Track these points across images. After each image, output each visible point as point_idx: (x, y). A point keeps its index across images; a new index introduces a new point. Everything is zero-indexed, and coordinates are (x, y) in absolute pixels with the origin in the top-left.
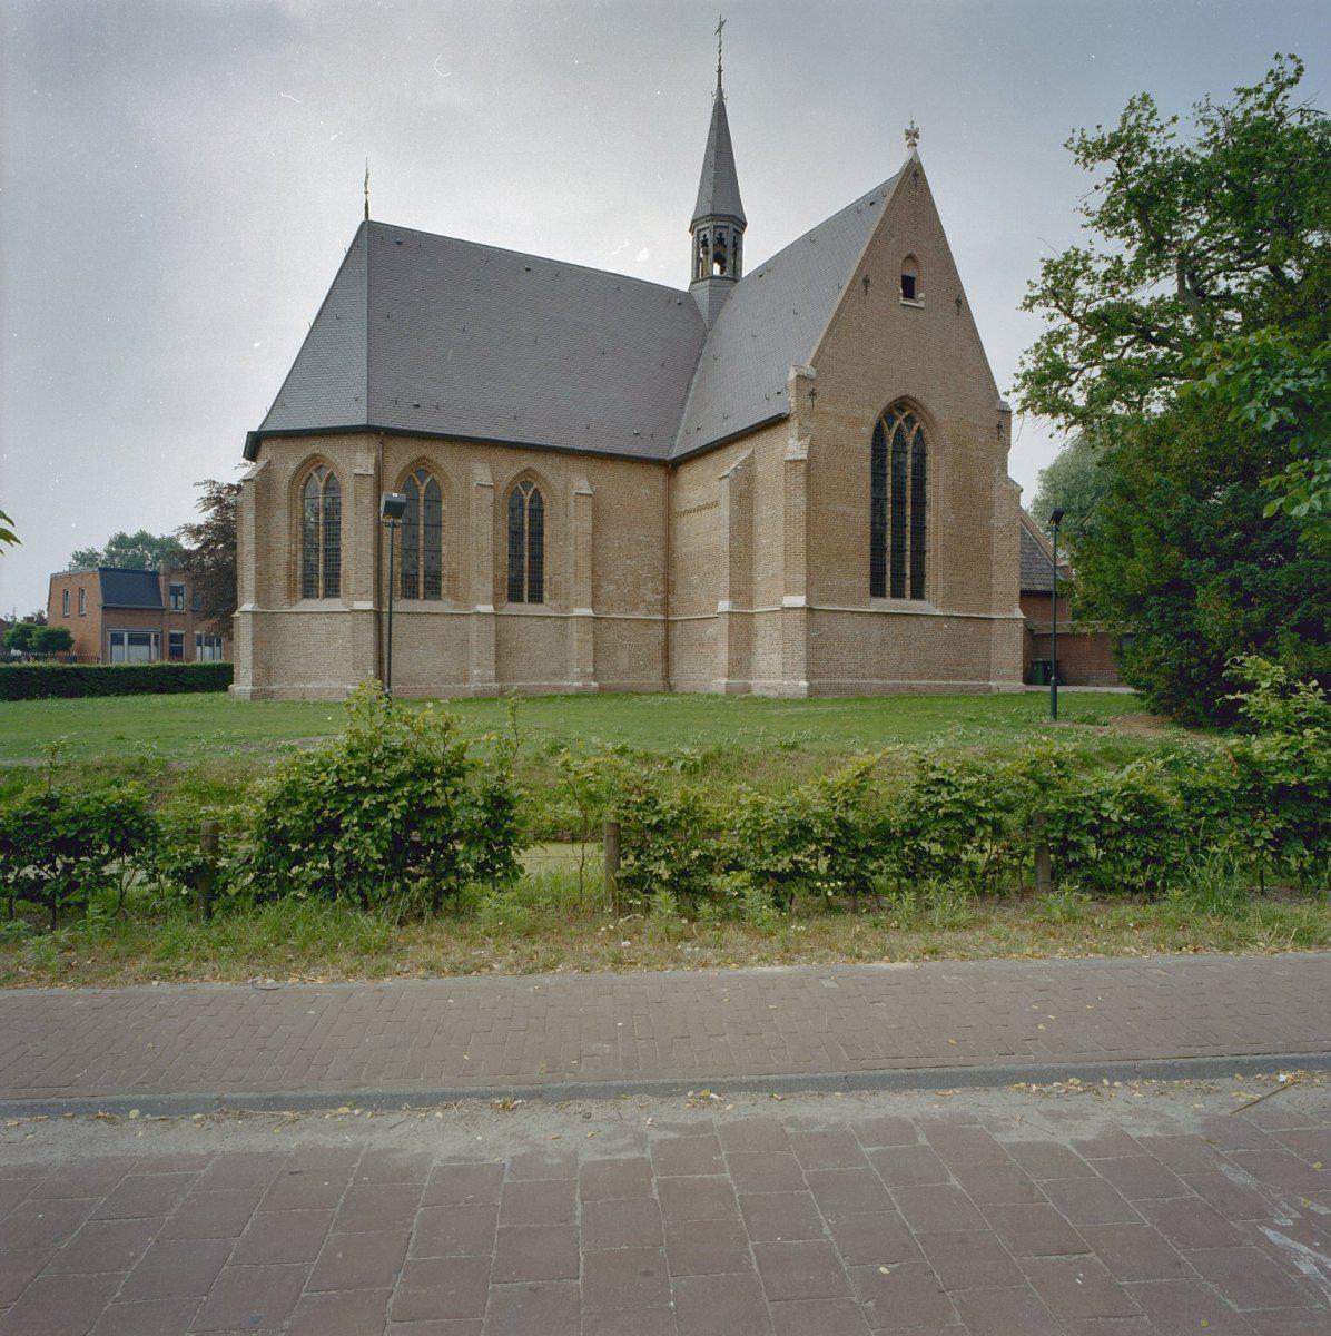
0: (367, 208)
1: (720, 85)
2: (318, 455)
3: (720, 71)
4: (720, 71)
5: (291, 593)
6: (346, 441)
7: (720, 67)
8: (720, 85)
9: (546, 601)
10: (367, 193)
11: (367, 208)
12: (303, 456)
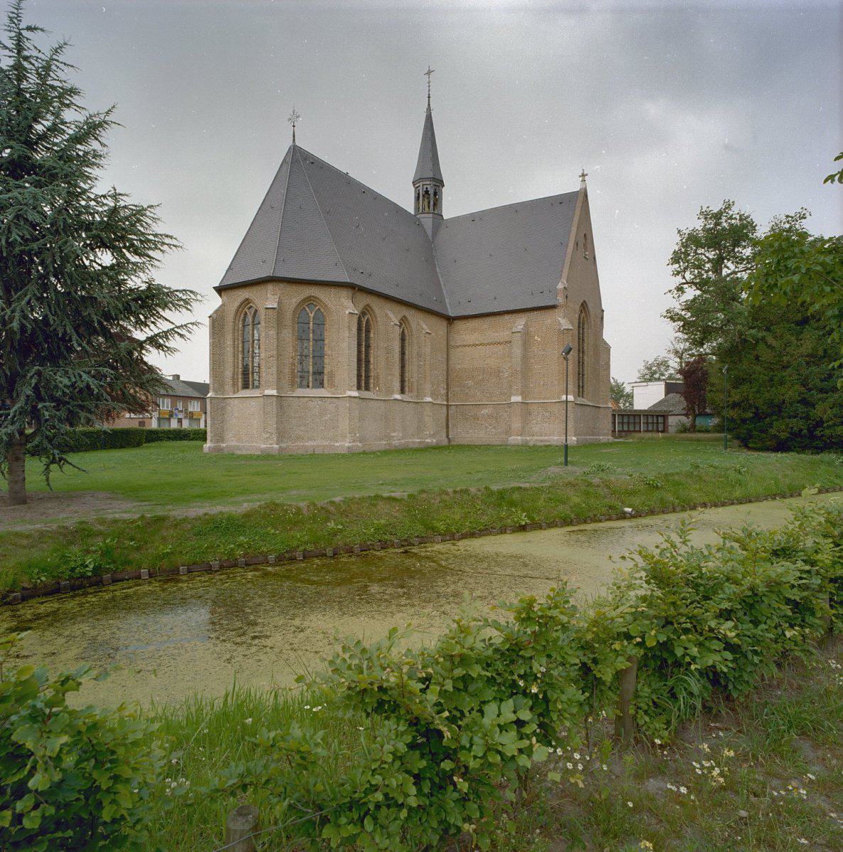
0: (294, 136)
1: (429, 105)
2: (313, 297)
3: (429, 97)
4: (429, 97)
5: (293, 384)
6: (326, 288)
7: (429, 94)
8: (429, 105)
9: (407, 393)
10: (294, 126)
11: (294, 136)
12: (303, 296)
